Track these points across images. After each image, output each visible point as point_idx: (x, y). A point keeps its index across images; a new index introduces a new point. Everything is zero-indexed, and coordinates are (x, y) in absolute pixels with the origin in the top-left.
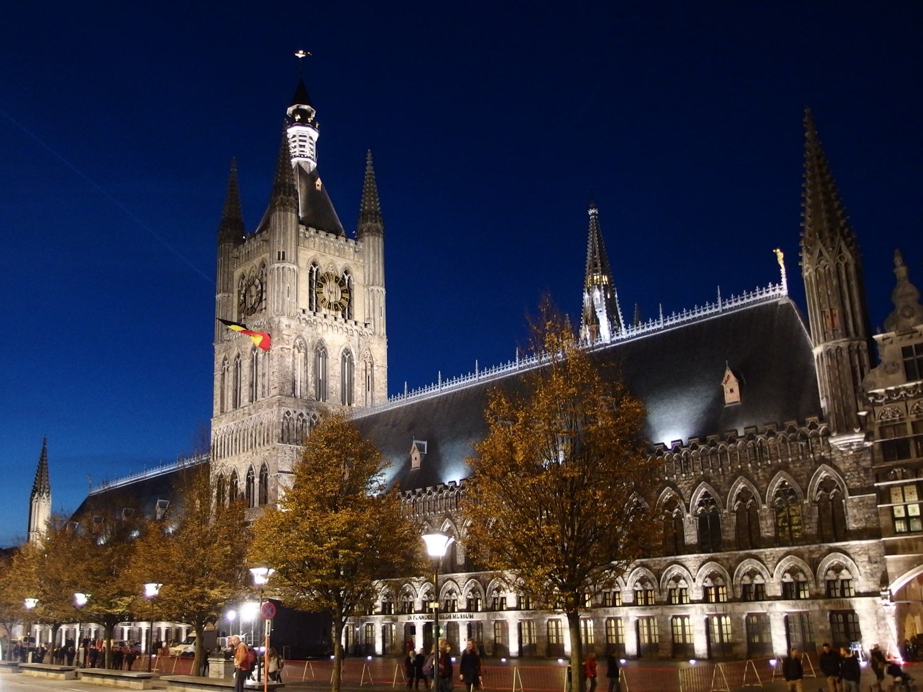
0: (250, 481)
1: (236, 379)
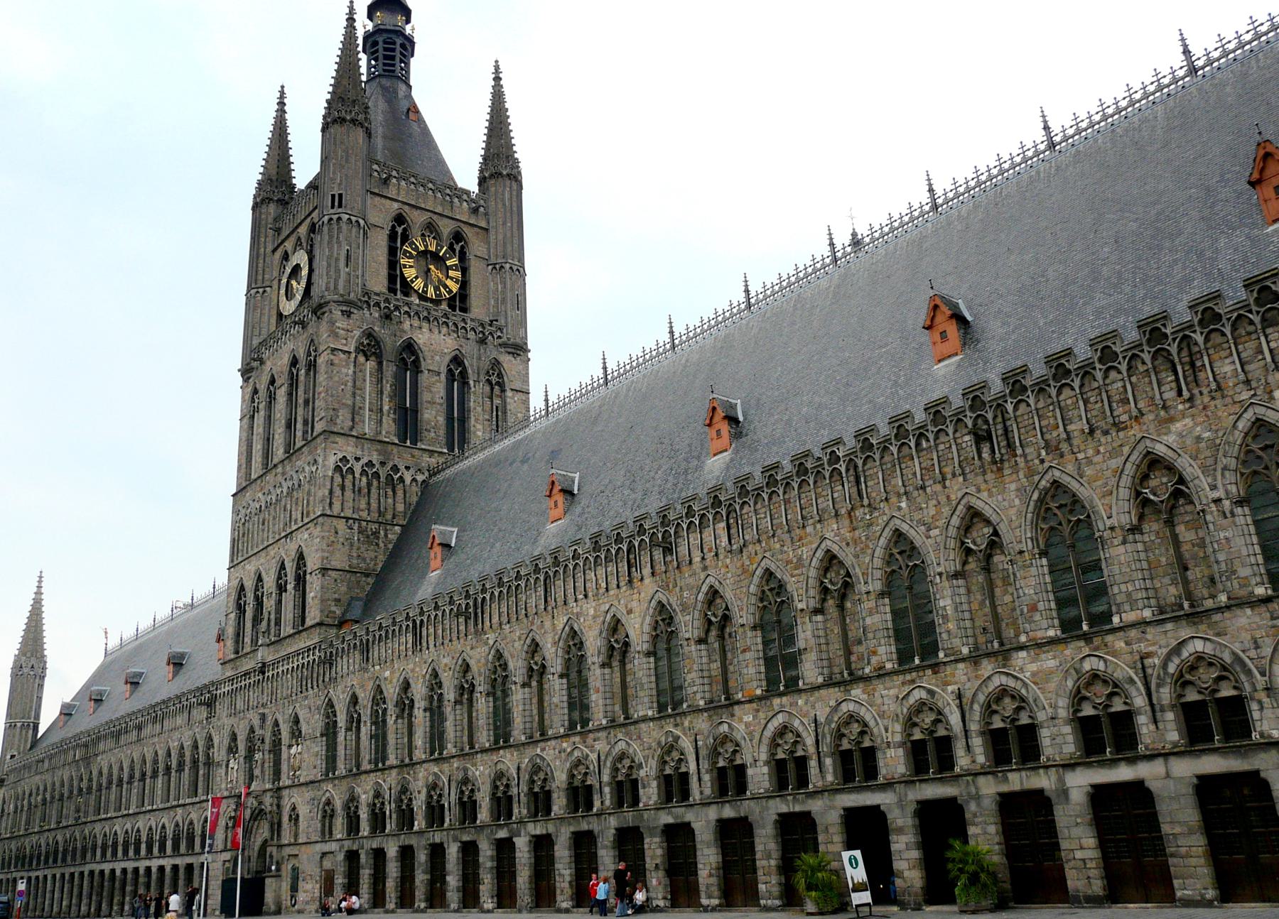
0: (281, 589)
1: (269, 418)
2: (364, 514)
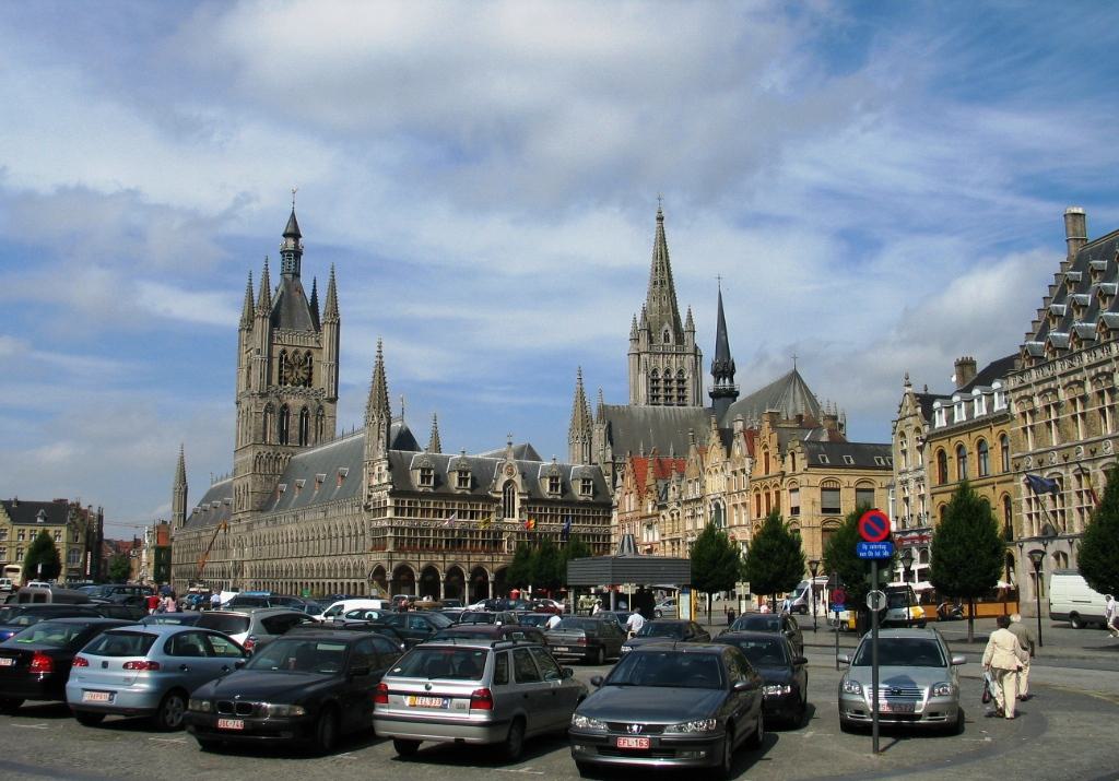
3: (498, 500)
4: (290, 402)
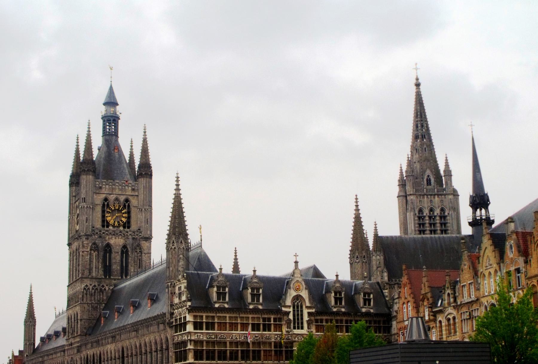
0: (75, 321)
2: (93, 302)
3: (288, 313)
4: (112, 242)
